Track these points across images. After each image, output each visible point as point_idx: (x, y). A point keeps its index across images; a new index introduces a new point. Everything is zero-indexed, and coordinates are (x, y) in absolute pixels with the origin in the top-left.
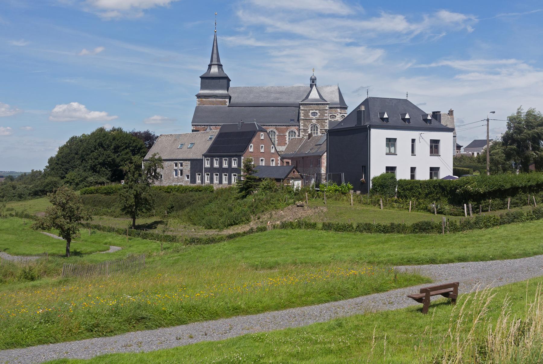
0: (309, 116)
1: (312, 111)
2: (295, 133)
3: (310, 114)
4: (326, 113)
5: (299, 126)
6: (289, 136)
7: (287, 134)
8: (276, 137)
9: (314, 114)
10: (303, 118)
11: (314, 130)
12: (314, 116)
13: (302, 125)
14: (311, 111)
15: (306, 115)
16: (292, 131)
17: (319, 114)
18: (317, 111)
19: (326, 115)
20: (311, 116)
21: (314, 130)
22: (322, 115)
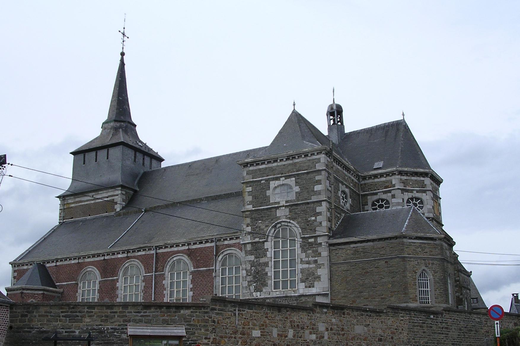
1: (277, 183)
4: (319, 182)
8: (189, 278)
10: (250, 207)
17: (297, 189)
18: (292, 181)
19: (317, 188)
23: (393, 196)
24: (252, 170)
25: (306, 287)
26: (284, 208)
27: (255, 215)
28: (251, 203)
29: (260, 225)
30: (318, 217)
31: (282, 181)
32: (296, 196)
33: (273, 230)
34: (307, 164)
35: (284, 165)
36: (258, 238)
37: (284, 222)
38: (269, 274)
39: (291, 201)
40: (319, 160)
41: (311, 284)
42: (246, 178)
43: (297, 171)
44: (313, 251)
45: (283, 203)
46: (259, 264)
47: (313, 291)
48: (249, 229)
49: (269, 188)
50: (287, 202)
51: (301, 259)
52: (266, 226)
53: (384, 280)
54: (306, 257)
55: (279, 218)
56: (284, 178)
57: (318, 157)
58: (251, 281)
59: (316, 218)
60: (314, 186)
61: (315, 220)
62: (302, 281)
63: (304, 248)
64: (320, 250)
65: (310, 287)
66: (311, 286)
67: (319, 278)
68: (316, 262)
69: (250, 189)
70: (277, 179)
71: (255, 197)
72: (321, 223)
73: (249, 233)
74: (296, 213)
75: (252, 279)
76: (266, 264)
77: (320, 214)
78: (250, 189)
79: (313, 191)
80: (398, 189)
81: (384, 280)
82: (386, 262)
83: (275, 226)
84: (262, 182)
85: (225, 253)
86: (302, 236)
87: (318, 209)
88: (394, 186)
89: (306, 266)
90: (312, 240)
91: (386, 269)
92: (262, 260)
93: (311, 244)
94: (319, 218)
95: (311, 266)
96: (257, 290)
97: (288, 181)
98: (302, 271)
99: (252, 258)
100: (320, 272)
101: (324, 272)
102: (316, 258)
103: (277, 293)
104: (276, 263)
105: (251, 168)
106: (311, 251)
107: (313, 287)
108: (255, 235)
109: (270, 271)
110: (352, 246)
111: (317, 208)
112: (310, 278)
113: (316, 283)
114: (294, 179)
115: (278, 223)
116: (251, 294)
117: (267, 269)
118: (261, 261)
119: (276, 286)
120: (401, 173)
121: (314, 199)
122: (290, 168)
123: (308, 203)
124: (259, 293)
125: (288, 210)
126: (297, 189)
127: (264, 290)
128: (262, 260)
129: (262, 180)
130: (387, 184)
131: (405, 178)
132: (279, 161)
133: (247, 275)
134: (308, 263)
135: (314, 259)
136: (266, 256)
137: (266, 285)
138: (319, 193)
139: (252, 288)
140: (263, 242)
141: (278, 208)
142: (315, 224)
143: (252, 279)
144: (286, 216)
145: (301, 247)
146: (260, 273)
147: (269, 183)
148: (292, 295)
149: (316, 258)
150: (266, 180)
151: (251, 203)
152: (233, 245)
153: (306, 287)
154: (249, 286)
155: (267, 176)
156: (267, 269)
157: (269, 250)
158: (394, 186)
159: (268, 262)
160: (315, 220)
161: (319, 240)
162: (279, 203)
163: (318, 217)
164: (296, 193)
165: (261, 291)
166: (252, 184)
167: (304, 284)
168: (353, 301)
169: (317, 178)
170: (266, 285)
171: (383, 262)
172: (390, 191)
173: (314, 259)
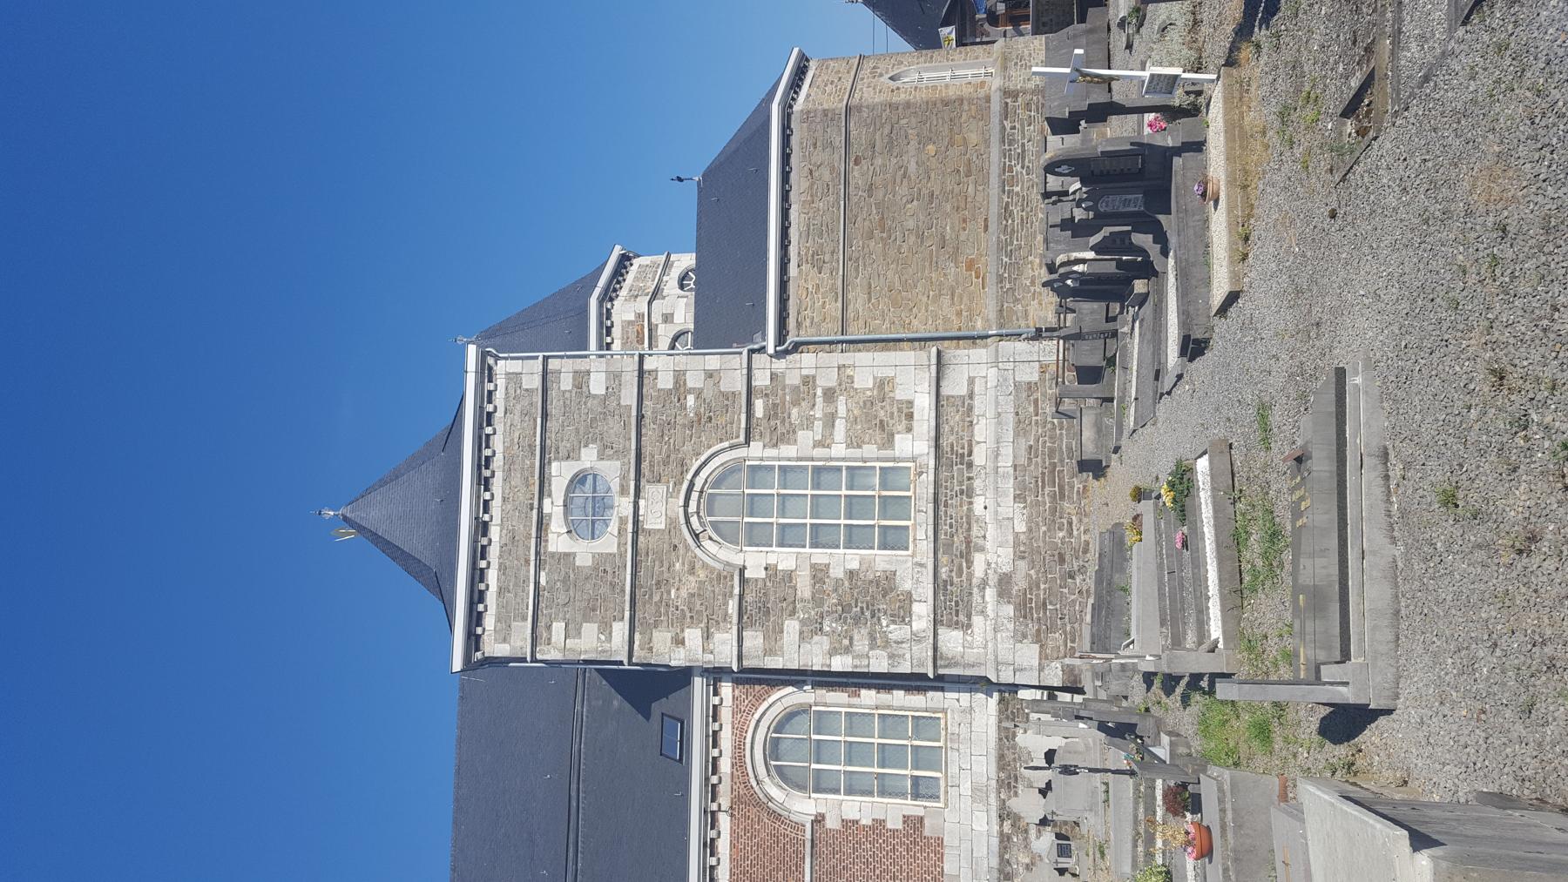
0: (603, 567)
1: (557, 526)
2: (790, 716)
3: (585, 552)
4: (581, 378)
5: (716, 674)
6: (821, 784)
7: (803, 807)
9: (588, 504)
10: (620, 630)
11: (753, 505)
12: (600, 506)
13: (693, 636)
14: (558, 540)
15: (585, 593)
16: (774, 749)
17: (589, 457)
18: (561, 473)
19: (597, 385)
20: (608, 543)
21: (753, 505)
22: (593, 422)
23: (668, 318)
24: (498, 620)
25: (909, 430)
26: (642, 503)
27: (646, 613)
28: (605, 628)
29: (684, 593)
30: (690, 384)
31: (553, 507)
32: (610, 458)
33: (707, 544)
34: (517, 418)
35: (504, 499)
36: (726, 604)
37: (686, 505)
38: (855, 565)
39: (624, 478)
40: (514, 378)
41: (900, 410)
42: (519, 644)
43: (533, 454)
44: (796, 403)
45: (624, 506)
46: (817, 600)
47: (924, 404)
48: (693, 636)
49: (569, 557)
50: (623, 491)
51: (817, 444)
52: (692, 570)
53: (912, 167)
54: (810, 427)
55: (672, 523)
56: (547, 502)
57: (501, 381)
58: (873, 638)
59: (690, 391)
60: (589, 395)
61: (699, 394)
62: (889, 442)
63: (782, 436)
64: (793, 379)
65: (910, 416)
66: (907, 413)
67: (882, 384)
68: (830, 395)
69: (558, 627)
70: (542, 524)
71: (589, 613)
72: (710, 375)
73: (707, 636)
74: (666, 463)
75: (864, 631)
76: (819, 574)
77: (679, 376)
78: (558, 627)
79: (606, 397)
80: (650, 303)
81: (912, 167)
82: (857, 162)
83: (696, 536)
84: (543, 582)
85: (761, 770)
86: (742, 439)
87: (665, 382)
88: (640, 316)
89: (840, 426)
90: (759, 406)
91: (879, 161)
92: (804, 587)
93: (773, 412)
94: (694, 380)
95: (842, 410)
96: (902, 614)
97: (558, 486)
98: (854, 442)
99: (792, 627)
100: (864, 381)
101: (867, 367)
102: (819, 392)
103: (921, 535)
104: (820, 538)
105: (489, 621)
106: (795, 412)
107: (910, 403)
108: (718, 615)
109: (843, 560)
110: (793, 270)
111: (660, 386)
112: (881, 415)
113: (900, 394)
114: (555, 465)
115: (688, 522)
116: (916, 638)
117: (837, 572)
118: (807, 594)
119: (893, 539)
120: (609, 295)
121: (629, 397)
122: (517, 480)
123: (640, 417)
124: (916, 607)
125: (649, 490)
126: (589, 457)
127: (907, 586)
128: (804, 587)
129: (537, 583)
130: (633, 337)
131: (623, 293)
132: (486, 517)
133: (848, 650)
134: (830, 420)
135: (819, 400)
136: (789, 575)
137: (890, 576)
138: (615, 377)
139: (896, 632)
140: (743, 580)
141: (636, 522)
142: (708, 394)
143: (864, 631)
144: (669, 495)
145: (775, 445)
146: (847, 599)
147: (553, 555)
148: (931, 477)
149: (819, 392)
150: (539, 567)
151: (605, 628)
152: (739, 731)
153: (909, 430)
154: (887, 644)
155: (527, 562)
156: (837, 572)
157: (772, 560)
158: (640, 316)
159: (813, 566)
160: (699, 394)
161: (761, 379)
162: (623, 521)
163: (690, 384)
164: (601, 457)
165: (909, 597)
166: (542, 624)
167: (897, 437)
168: (969, 268)
169: (566, 383)
170: (890, 576)
171: (856, 172)
172: (652, 330)
173: (819, 400)
